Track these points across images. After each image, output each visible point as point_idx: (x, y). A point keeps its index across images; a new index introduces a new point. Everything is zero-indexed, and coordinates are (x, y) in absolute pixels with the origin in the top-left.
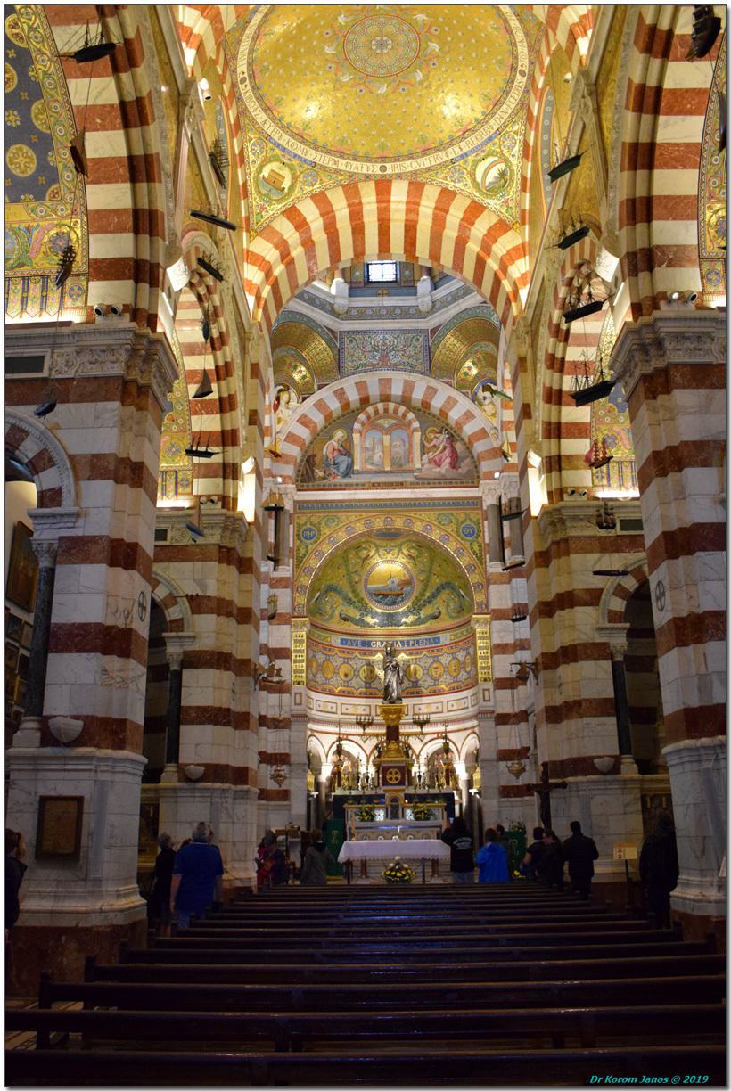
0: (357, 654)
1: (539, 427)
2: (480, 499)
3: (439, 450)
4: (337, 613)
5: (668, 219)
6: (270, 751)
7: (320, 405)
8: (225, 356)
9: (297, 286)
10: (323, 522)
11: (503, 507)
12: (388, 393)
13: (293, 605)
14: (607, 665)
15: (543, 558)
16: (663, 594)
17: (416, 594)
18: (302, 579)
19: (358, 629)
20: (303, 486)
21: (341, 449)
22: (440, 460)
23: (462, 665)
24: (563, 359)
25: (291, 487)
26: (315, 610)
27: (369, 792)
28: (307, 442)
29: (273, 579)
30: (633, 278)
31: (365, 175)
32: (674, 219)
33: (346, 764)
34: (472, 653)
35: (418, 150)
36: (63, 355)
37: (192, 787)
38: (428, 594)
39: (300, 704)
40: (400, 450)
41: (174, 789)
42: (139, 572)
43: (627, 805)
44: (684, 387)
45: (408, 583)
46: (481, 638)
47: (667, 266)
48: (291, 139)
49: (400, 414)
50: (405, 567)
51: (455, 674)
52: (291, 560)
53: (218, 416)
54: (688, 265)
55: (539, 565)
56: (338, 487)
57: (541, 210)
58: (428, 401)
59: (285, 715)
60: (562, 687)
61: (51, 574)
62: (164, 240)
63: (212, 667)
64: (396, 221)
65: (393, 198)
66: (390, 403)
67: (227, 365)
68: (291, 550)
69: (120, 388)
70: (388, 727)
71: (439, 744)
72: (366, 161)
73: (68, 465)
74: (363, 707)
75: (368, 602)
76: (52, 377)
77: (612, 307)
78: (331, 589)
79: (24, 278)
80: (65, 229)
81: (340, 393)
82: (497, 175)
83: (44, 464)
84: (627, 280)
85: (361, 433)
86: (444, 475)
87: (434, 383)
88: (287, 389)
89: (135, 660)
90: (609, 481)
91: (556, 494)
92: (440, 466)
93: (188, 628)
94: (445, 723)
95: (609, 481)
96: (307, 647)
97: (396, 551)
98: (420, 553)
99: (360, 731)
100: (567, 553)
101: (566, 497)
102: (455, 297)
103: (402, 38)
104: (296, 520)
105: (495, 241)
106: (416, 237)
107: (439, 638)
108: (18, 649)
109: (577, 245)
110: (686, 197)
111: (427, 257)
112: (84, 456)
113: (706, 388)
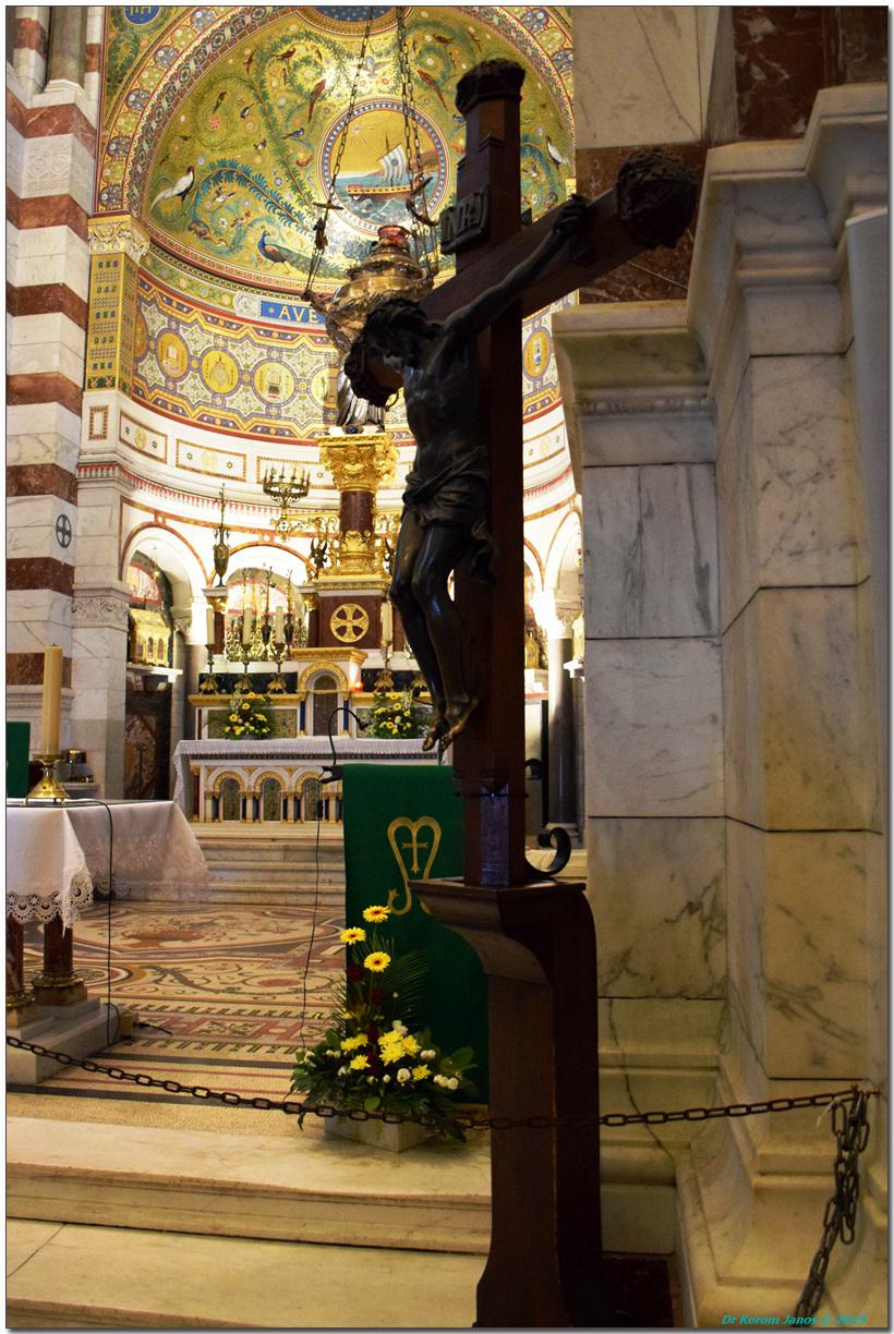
0: (304, 339)
4: (252, 239)
13: (96, 186)
18: (121, 122)
29: (33, 111)
39: (104, 436)
51: (538, 369)
68: (89, 50)
70: (345, 497)
78: (227, 173)
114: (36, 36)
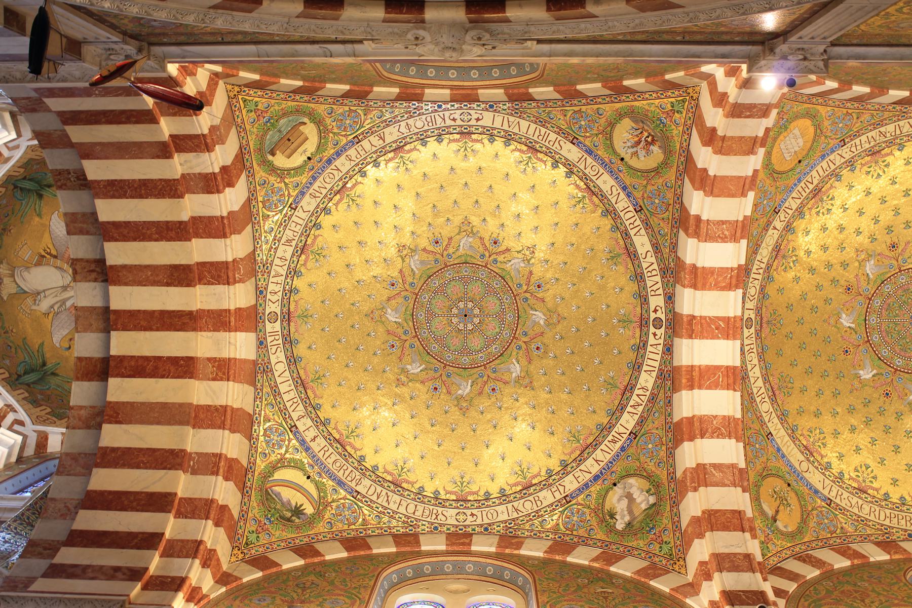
31: (266, 289)
35: (302, 372)
48: (341, 175)
72: (284, 290)
82: (294, 504)
103: (455, 343)
106: (163, 377)
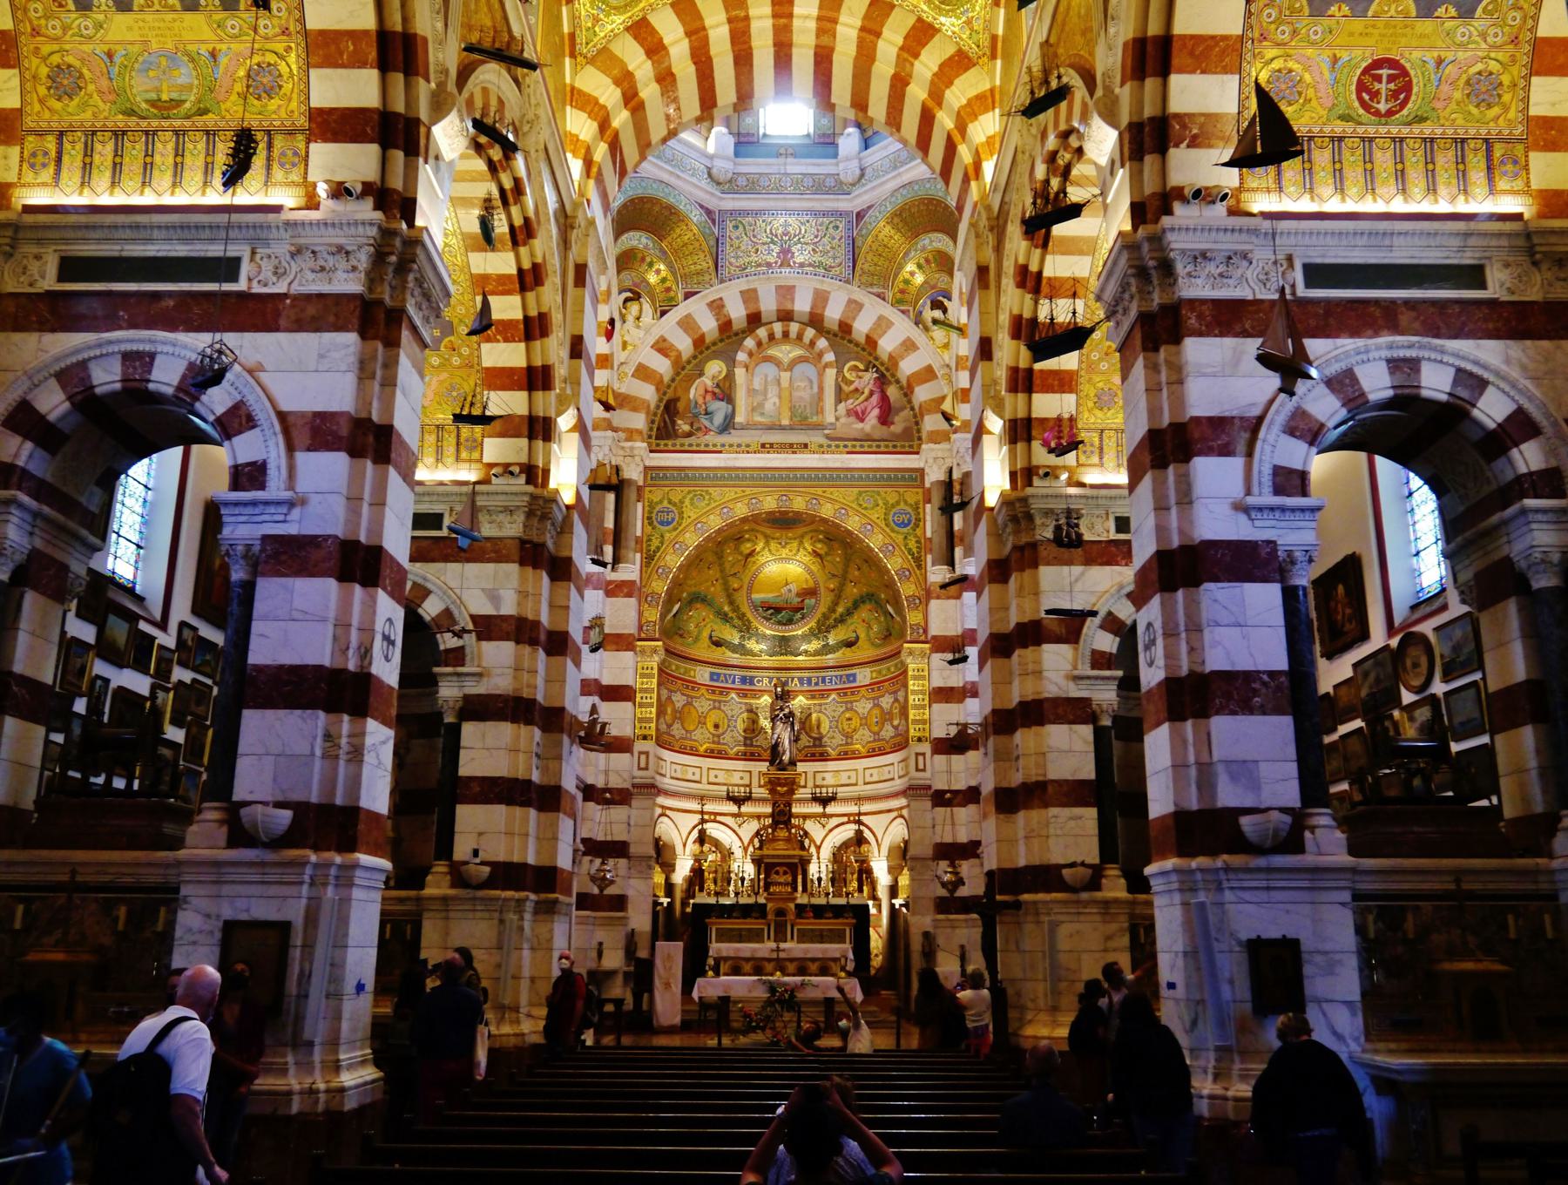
1: (1002, 374)
2: (921, 471)
3: (862, 398)
4: (706, 634)
5: (1193, 72)
6: (601, 838)
7: (687, 324)
8: (532, 255)
9: (649, 145)
10: (687, 502)
11: (957, 487)
12: (789, 307)
14: (1086, 731)
15: (998, 571)
16: (1153, 642)
17: (822, 609)
18: (654, 584)
19: (734, 658)
20: (658, 445)
21: (717, 390)
22: (863, 412)
23: (886, 717)
24: (1040, 273)
25: (641, 446)
26: (672, 631)
27: (743, 900)
28: (666, 379)
29: (610, 582)
30: (1136, 164)
32: (1203, 72)
33: (711, 857)
34: (901, 699)
36: (270, 257)
37: (471, 896)
38: (840, 610)
40: (804, 394)
41: (445, 899)
42: (384, 589)
43: (1108, 938)
44: (1200, 334)
45: (812, 592)
46: (915, 678)
47: (1188, 146)
49: (807, 339)
50: (810, 572)
51: (876, 729)
52: (638, 556)
53: (522, 345)
54: (1221, 144)
55: (992, 580)
56: (711, 448)
57: (1019, 38)
58: (849, 322)
59: (615, 782)
60: (1021, 762)
61: (249, 588)
62: (428, 81)
63: (505, 719)
64: (802, 46)
65: (797, 10)
66: (792, 324)
67: (536, 267)
68: (638, 541)
69: (357, 313)
71: (848, 832)
73: (277, 427)
74: (741, 774)
75: (752, 619)
76: (254, 291)
77: (1105, 207)
79: (207, 133)
80: (271, 58)
81: (717, 306)
83: (241, 424)
84: (1127, 165)
85: (747, 367)
86: (868, 435)
87: (859, 295)
88: (636, 297)
89: (375, 718)
90: (1101, 458)
91: (1023, 475)
92: (862, 420)
93: (472, 658)
94: (859, 800)
95: (1101, 458)
96: (659, 685)
97: (795, 544)
98: (831, 549)
99: (733, 808)
100: (1037, 567)
101: (1036, 482)
102: (896, 164)
104: (647, 495)
105: (950, 83)
107: (854, 675)
108: (210, 688)
109: (1064, 105)
110: (1225, 38)
111: (848, 104)
112: (302, 414)
113: (1236, 335)
114: (611, 538)
